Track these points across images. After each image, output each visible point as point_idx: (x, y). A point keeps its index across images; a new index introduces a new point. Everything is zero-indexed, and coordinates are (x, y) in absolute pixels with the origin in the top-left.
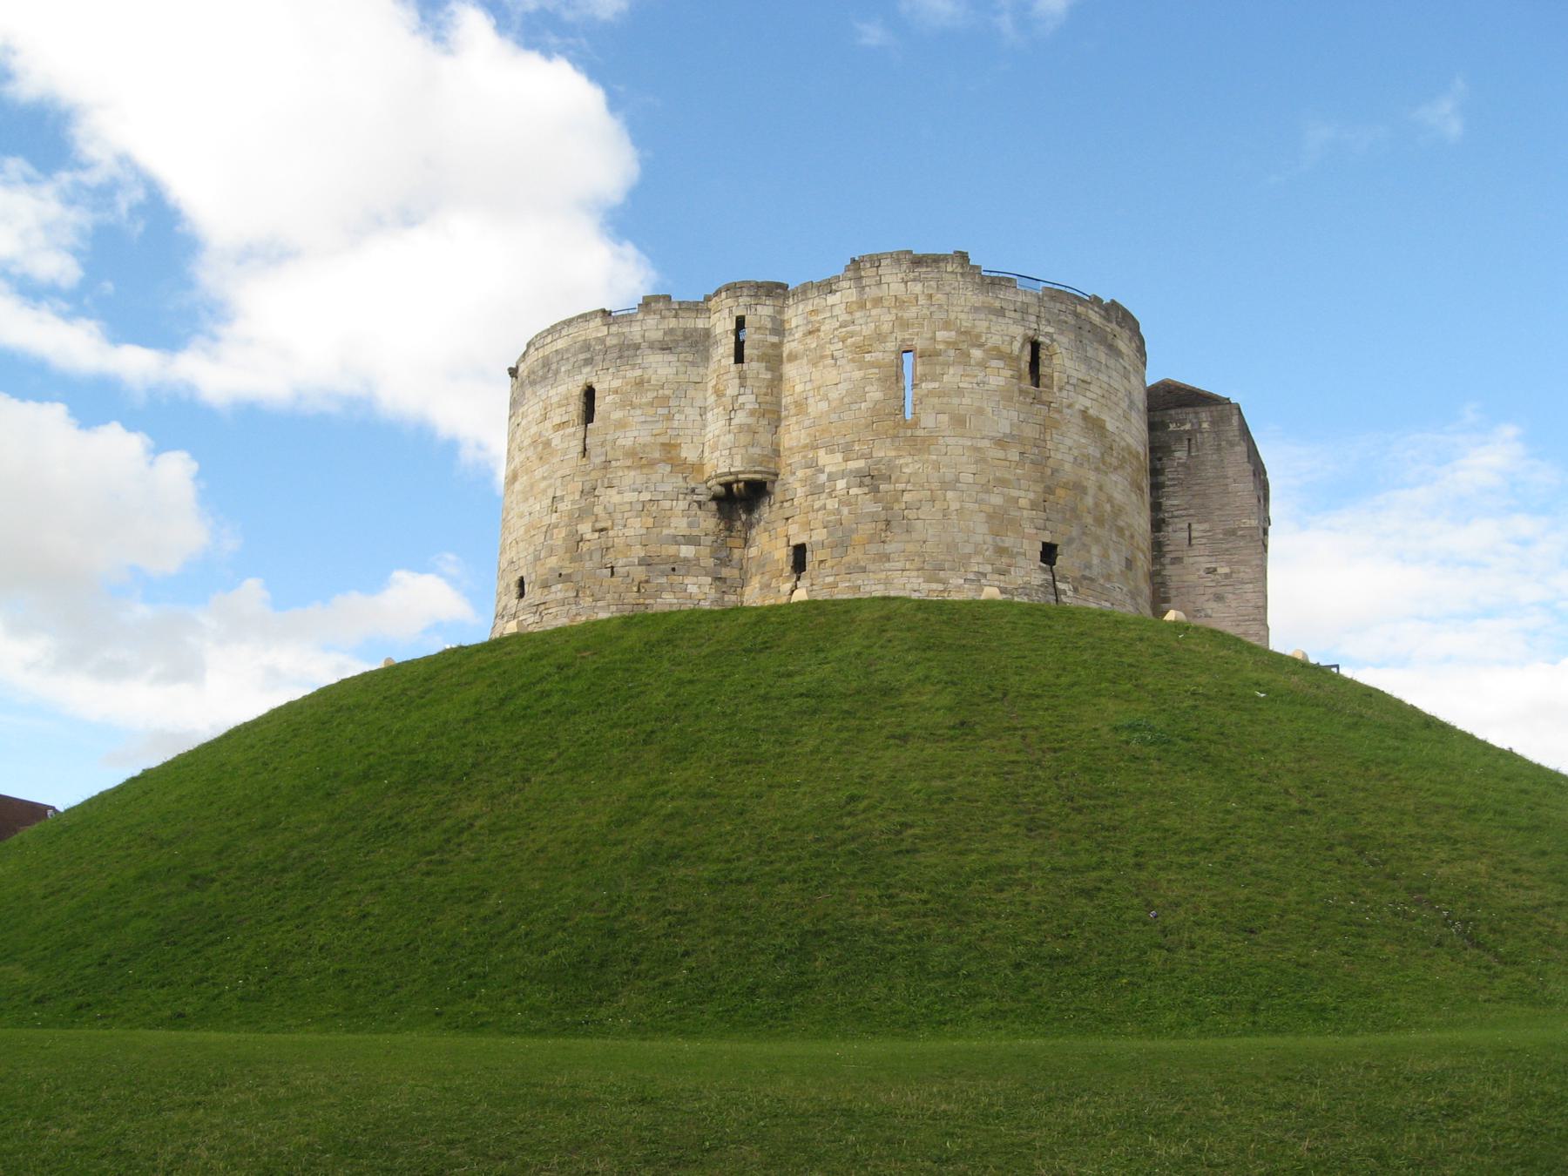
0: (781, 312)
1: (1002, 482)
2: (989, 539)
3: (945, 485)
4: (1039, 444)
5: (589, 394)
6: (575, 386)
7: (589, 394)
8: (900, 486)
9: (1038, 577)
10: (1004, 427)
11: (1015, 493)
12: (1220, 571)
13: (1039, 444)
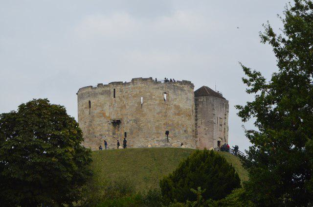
1: (158, 121)
2: (156, 132)
4: (166, 112)
5: (90, 102)
6: (87, 101)
9: (165, 137)
10: (158, 111)
13: (166, 112)
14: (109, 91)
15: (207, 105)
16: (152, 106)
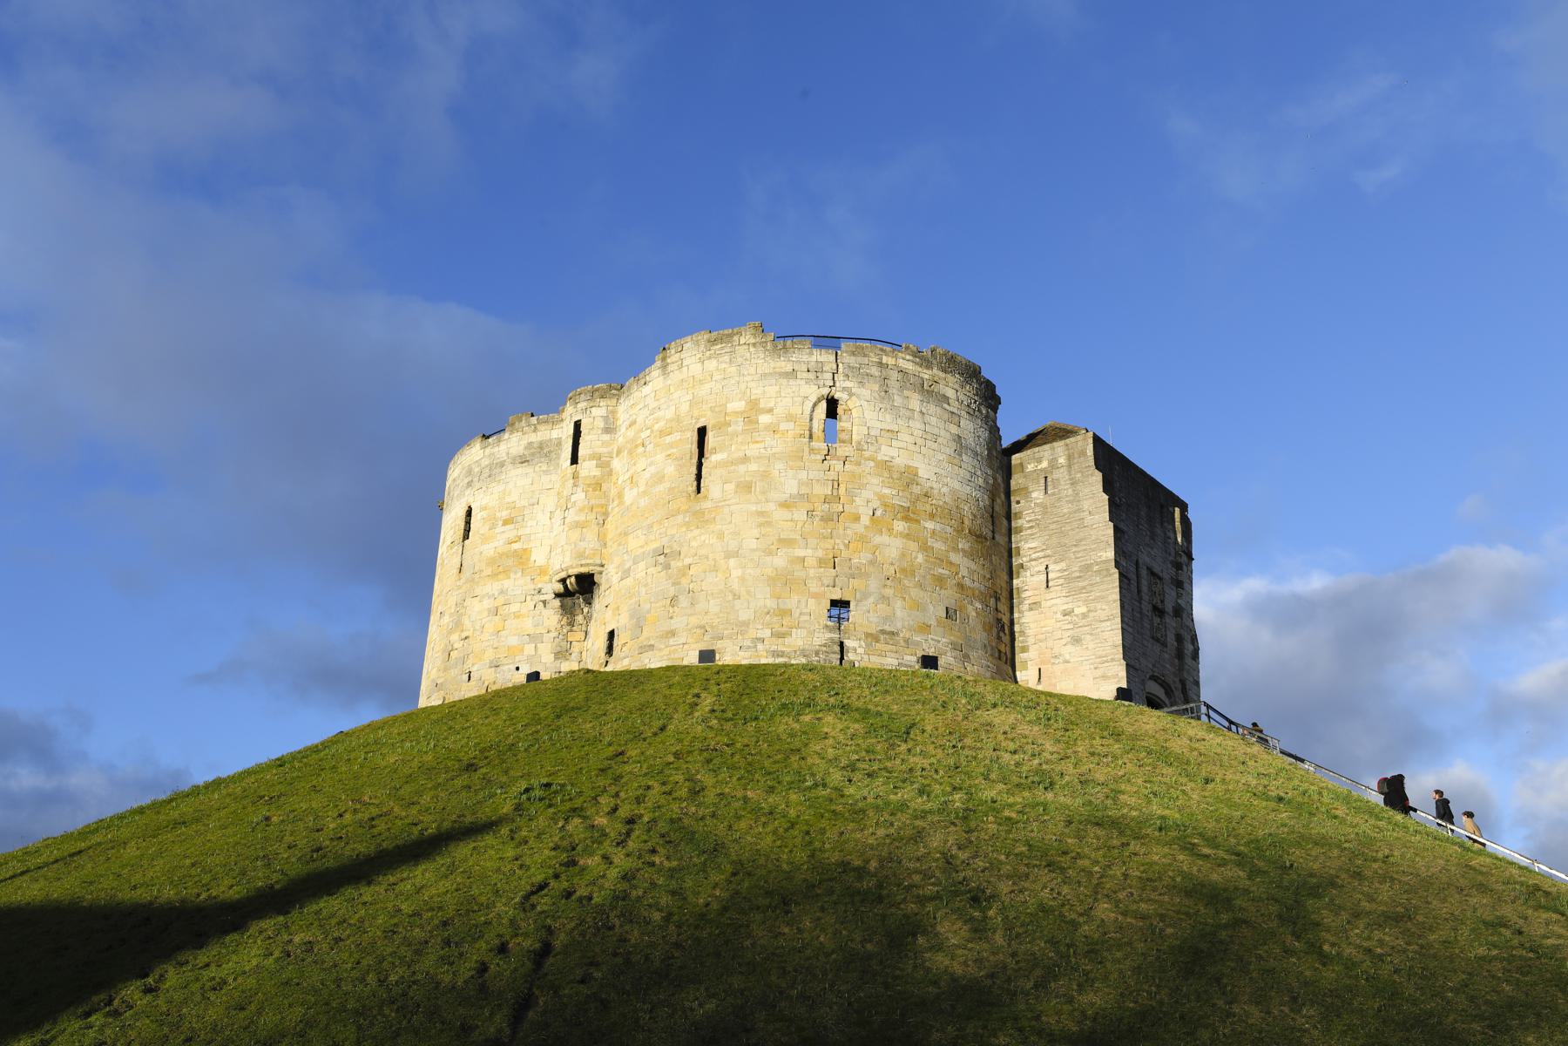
0: (614, 412)
1: (787, 542)
3: (729, 555)
5: (469, 513)
7: (469, 513)
8: (687, 561)
10: (791, 487)
11: (800, 553)
12: (1077, 611)
14: (559, 443)
15: (1074, 483)
16: (753, 467)
